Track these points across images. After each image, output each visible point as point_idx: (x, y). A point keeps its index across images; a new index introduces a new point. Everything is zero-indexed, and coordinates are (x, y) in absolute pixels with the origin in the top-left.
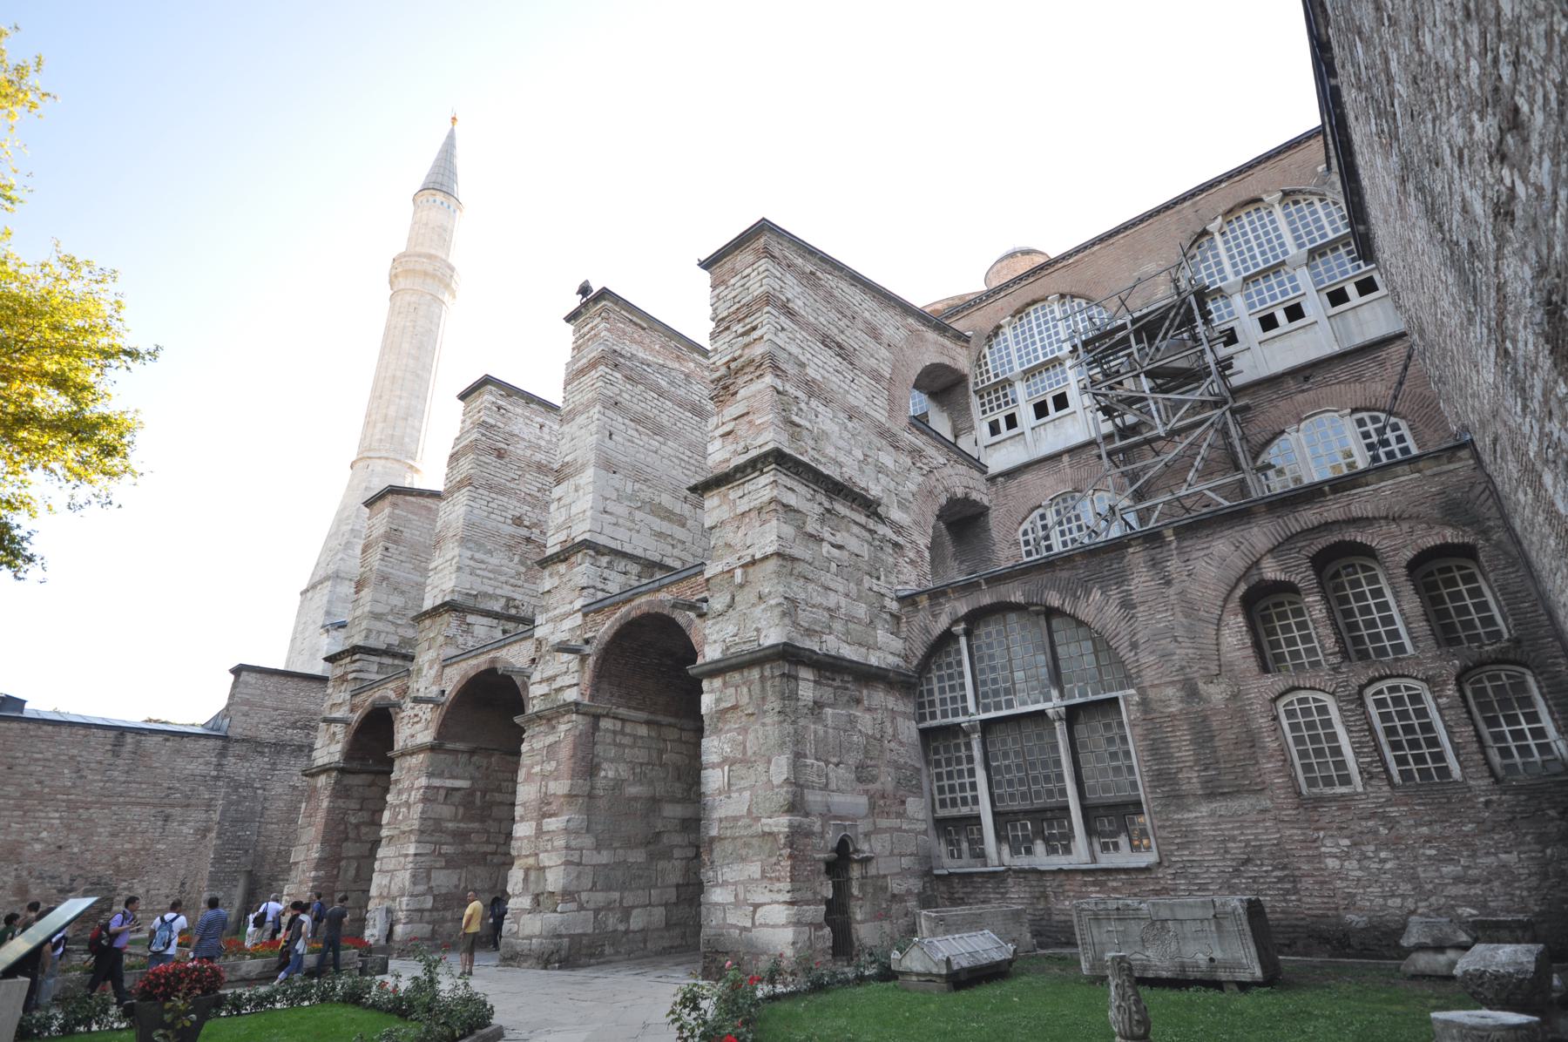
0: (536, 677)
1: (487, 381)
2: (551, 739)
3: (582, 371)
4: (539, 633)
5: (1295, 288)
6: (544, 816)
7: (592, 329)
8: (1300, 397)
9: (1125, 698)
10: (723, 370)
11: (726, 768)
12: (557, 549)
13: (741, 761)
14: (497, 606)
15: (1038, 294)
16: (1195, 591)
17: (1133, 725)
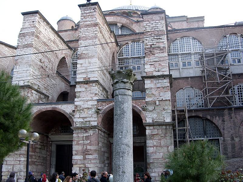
0: (77, 115)
1: (37, 12)
2: (87, 134)
3: (88, 25)
4: (76, 103)
5: (240, 56)
6: (86, 154)
7: (90, 12)
8: (238, 79)
9: (221, 139)
10: (149, 46)
11: (155, 148)
12: (82, 80)
13: (159, 146)
14: (36, 87)
15: (188, 35)
16: (236, 120)
17: (221, 144)
